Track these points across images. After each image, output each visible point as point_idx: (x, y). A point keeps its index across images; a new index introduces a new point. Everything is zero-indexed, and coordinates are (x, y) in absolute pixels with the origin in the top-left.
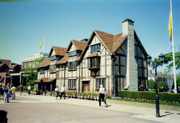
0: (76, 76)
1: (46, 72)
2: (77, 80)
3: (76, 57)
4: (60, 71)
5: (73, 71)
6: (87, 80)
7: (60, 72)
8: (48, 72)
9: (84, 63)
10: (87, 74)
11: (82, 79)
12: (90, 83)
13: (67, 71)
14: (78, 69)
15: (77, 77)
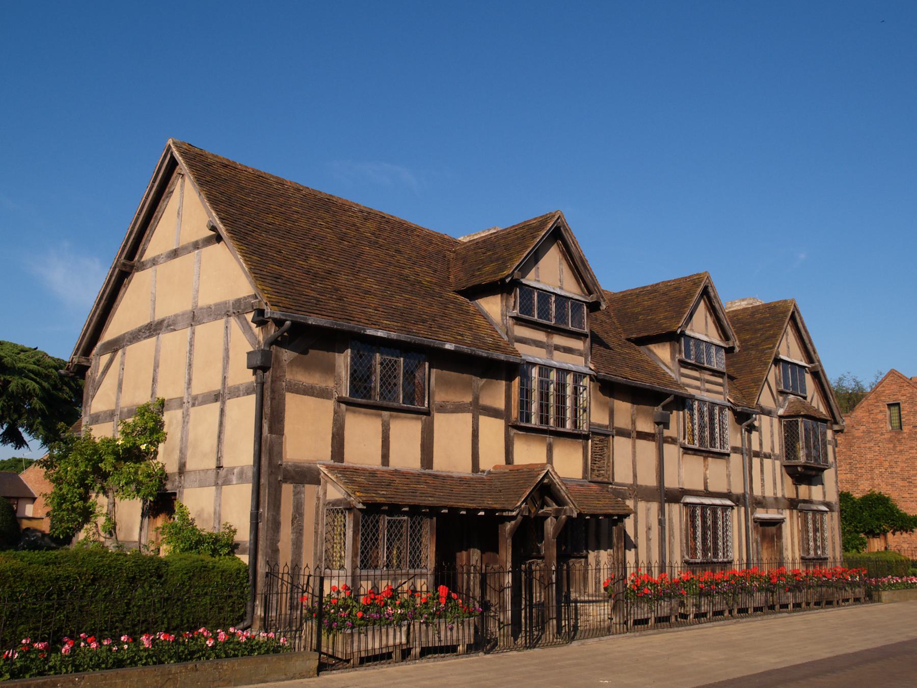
0: (725, 491)
1: (458, 408)
3: (720, 380)
4: (622, 433)
5: (710, 459)
7: (621, 447)
8: (479, 410)
10: (771, 480)
11: (752, 514)
12: (783, 525)
13: (671, 451)
14: (735, 450)
15: (728, 496)
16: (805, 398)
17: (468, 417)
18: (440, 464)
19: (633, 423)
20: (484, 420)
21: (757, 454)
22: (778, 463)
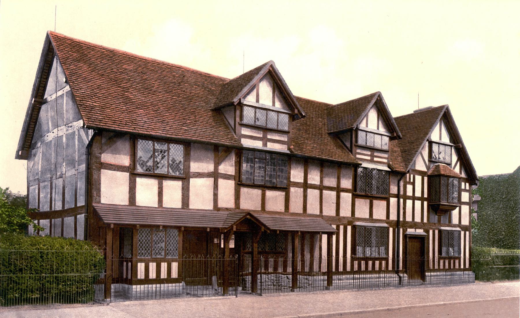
2: (391, 229)
6: (420, 232)
7: (313, 194)
9: (409, 183)
16: (449, 164)
17: (212, 180)
18: (195, 204)
19: (321, 181)
20: (221, 181)
21: (409, 198)
22: (425, 203)
